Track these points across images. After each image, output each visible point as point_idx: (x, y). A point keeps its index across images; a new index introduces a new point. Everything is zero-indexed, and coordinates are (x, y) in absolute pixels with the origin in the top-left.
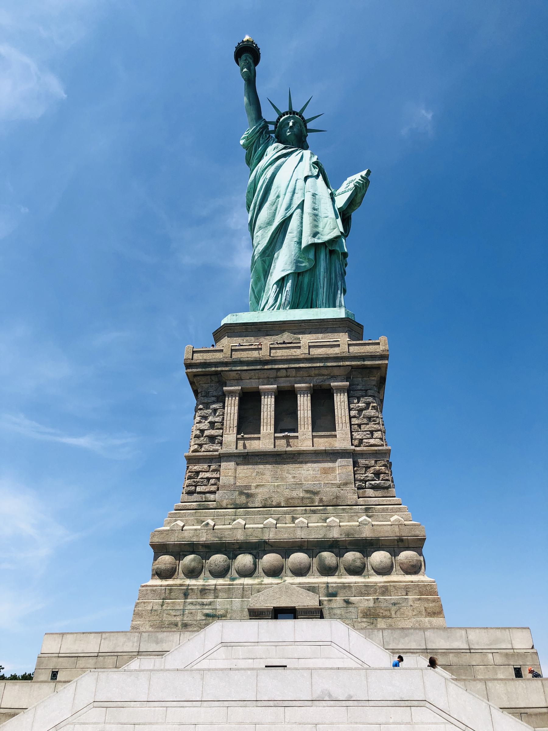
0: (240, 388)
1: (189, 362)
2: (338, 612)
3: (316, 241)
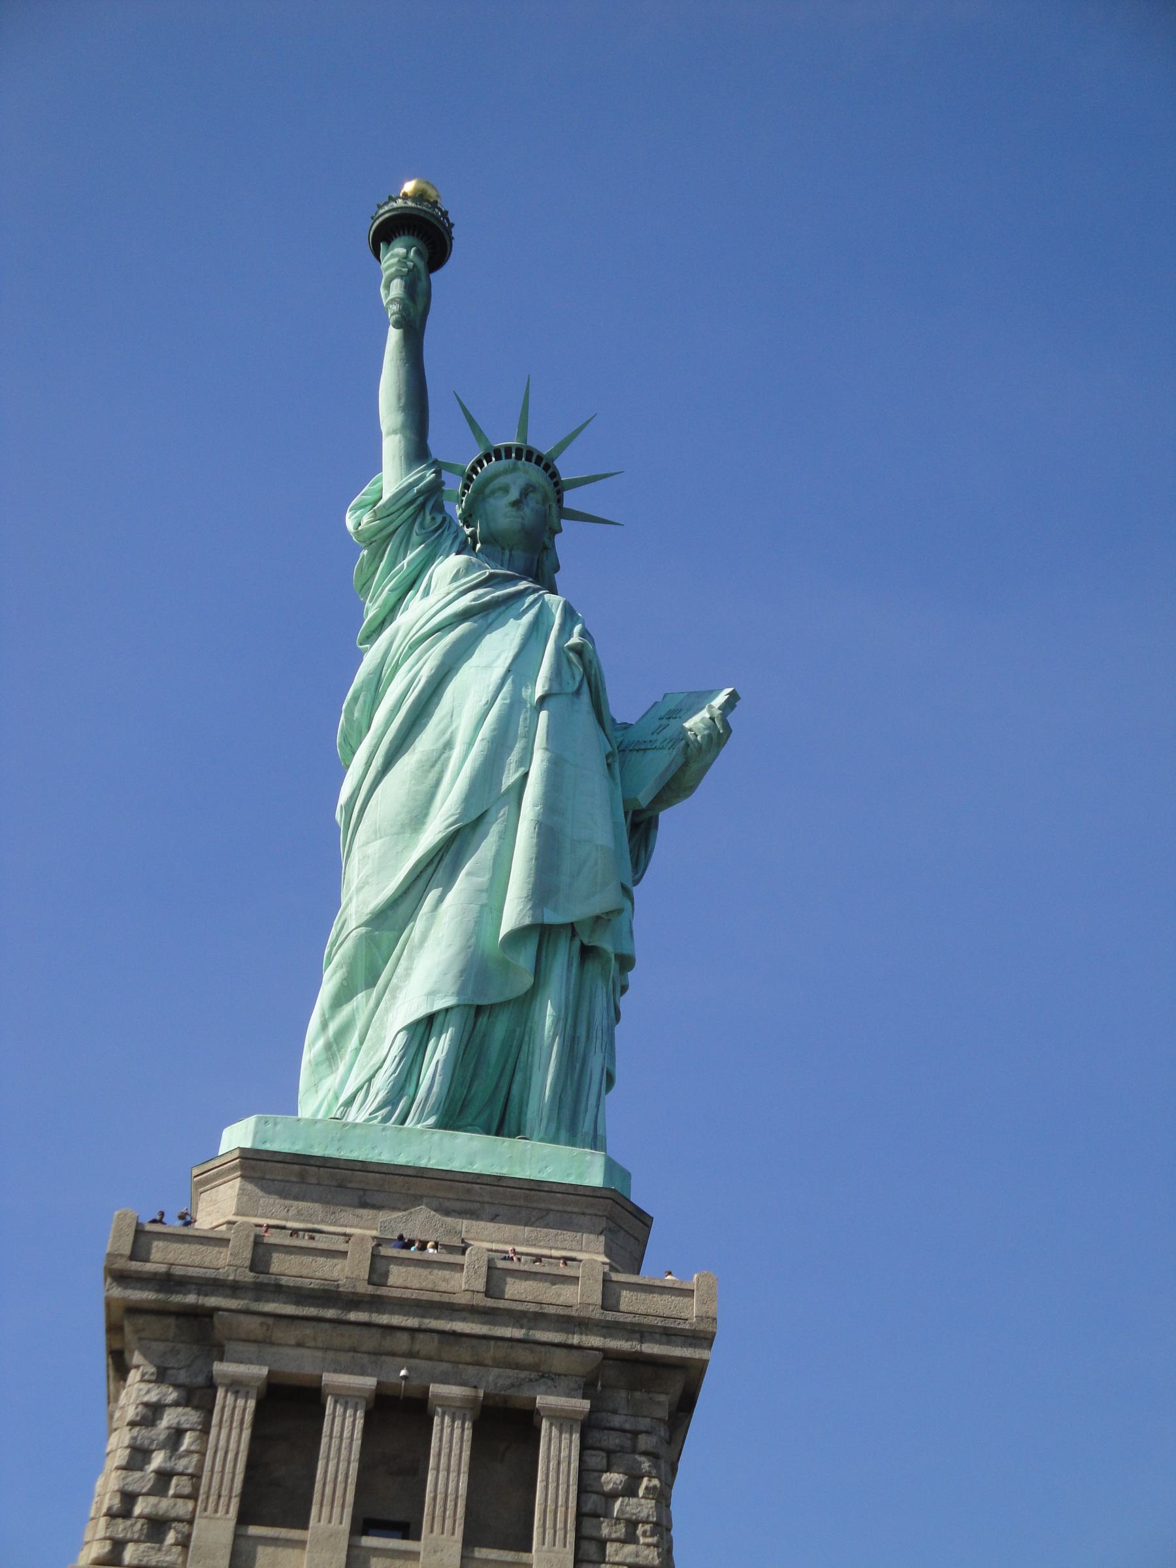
0: (264, 1371)
1: (122, 1264)
3: (552, 917)
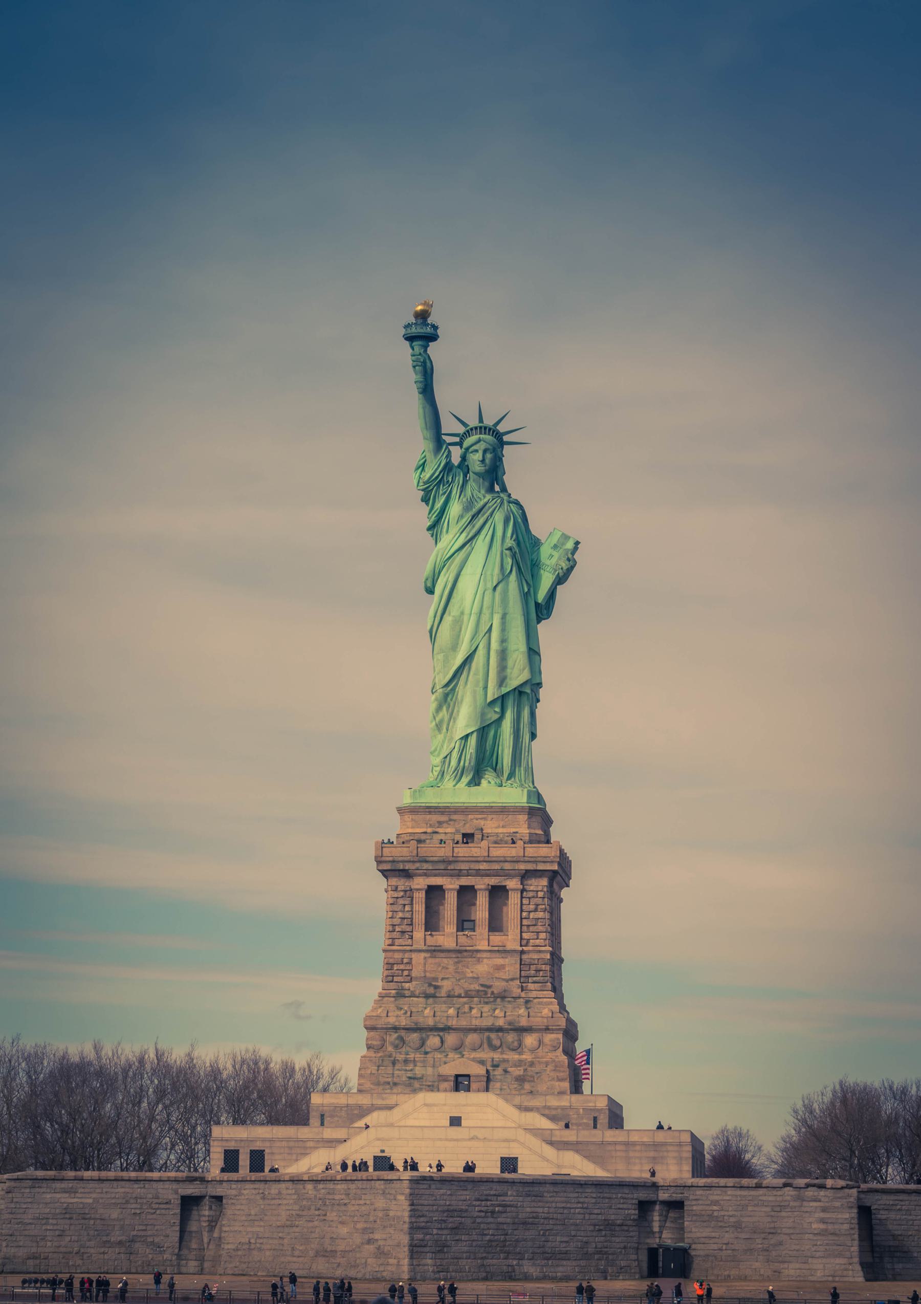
2: (499, 1077)
3: (505, 690)
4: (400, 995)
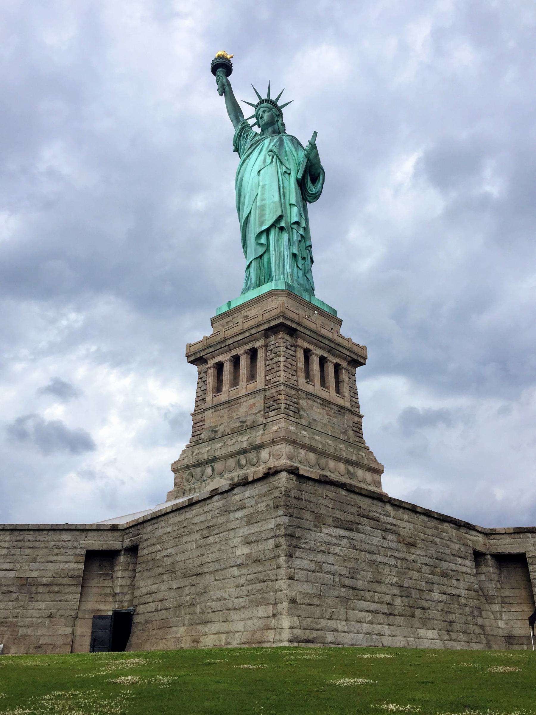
3: (264, 228)
4: (197, 443)
